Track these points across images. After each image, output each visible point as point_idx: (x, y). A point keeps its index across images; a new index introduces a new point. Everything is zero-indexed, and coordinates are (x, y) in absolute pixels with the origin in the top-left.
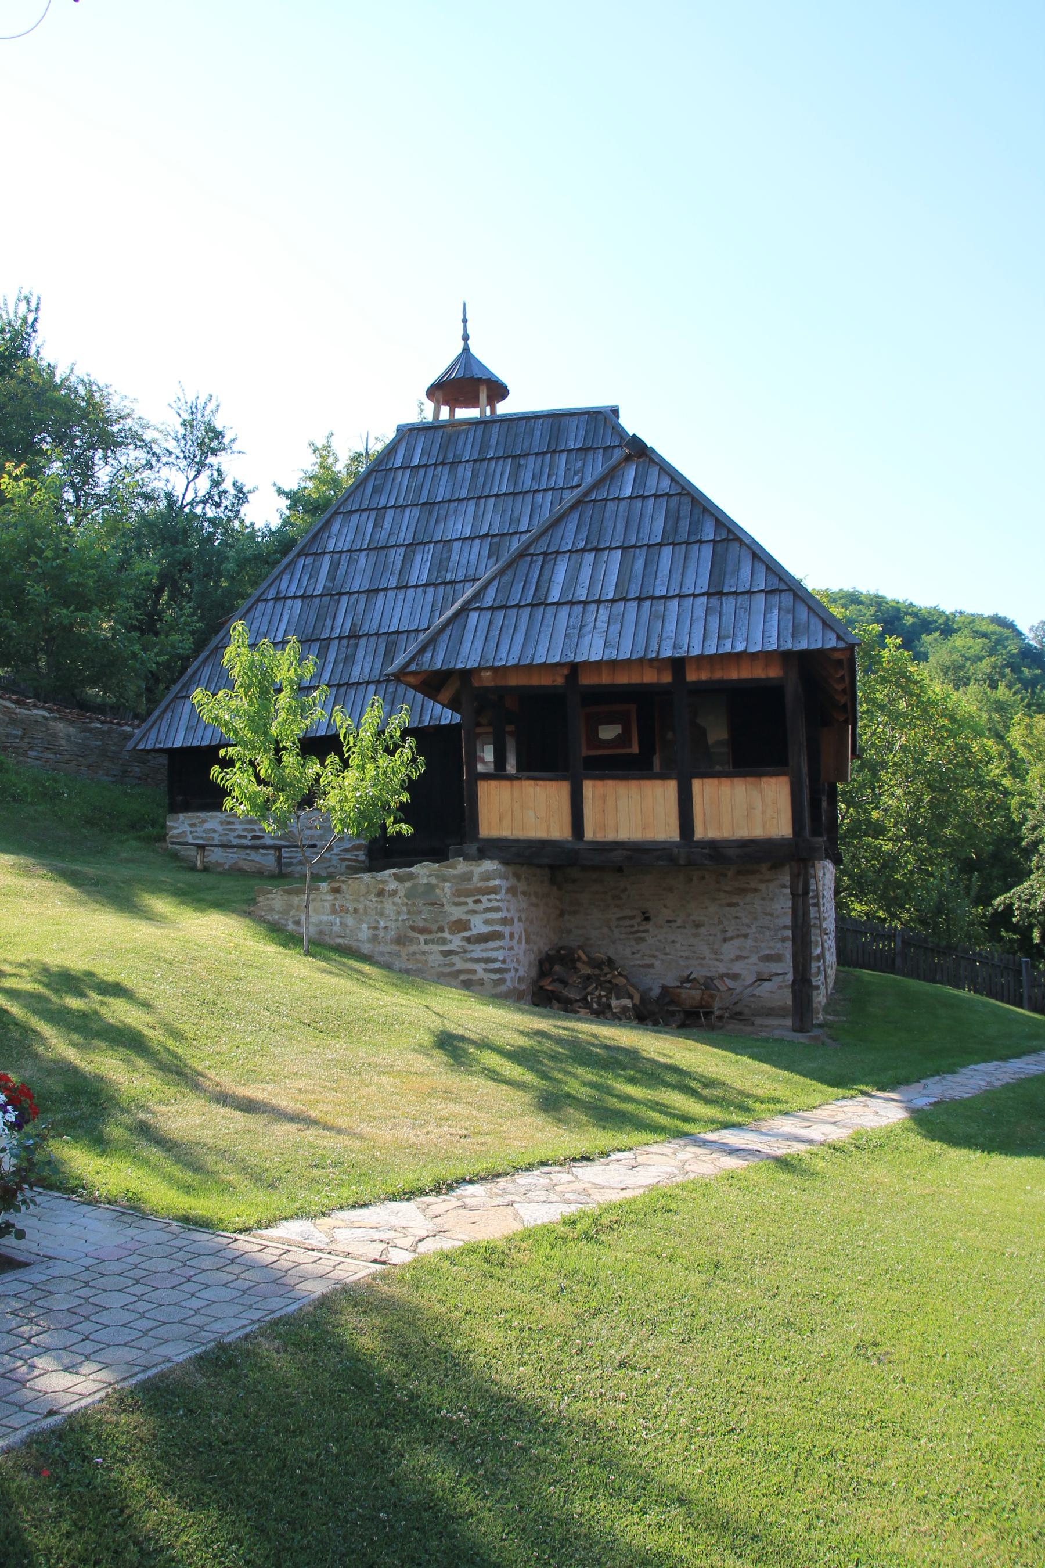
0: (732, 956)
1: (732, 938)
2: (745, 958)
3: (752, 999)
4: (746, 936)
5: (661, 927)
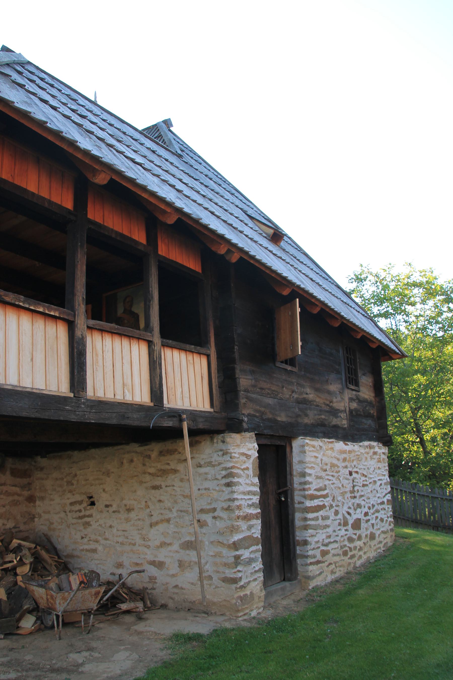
0: (157, 543)
1: (157, 523)
2: (170, 544)
3: (176, 590)
4: (168, 521)
5: (101, 512)
